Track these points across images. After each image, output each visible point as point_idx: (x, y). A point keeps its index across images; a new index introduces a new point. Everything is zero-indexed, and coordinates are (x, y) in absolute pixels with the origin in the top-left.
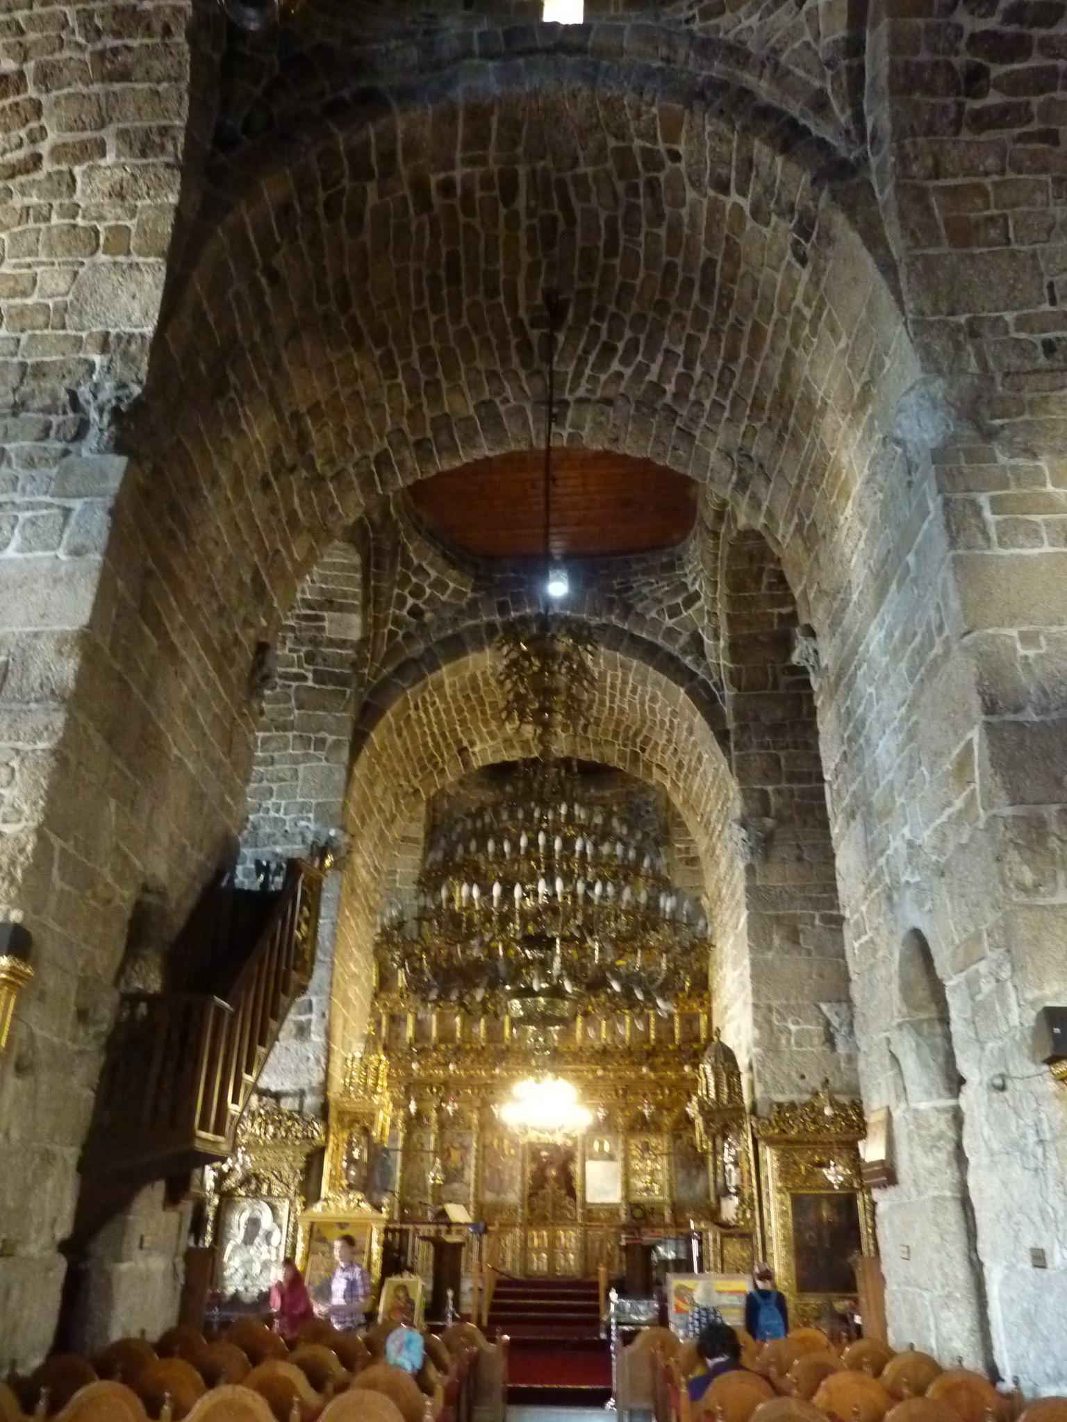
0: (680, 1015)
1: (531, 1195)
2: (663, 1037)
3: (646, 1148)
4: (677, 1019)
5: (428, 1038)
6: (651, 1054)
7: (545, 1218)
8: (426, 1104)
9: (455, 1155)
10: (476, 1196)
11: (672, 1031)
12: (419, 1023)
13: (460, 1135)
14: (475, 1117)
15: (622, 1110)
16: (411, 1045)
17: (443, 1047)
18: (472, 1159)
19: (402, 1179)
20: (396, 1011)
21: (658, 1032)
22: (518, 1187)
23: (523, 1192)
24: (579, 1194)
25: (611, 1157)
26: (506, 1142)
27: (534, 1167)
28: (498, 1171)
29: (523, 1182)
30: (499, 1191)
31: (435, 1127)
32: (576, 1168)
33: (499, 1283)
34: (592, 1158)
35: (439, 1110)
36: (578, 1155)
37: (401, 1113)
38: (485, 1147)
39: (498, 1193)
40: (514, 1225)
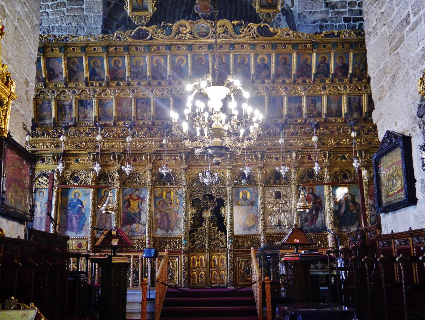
0: (307, 97)
1: (191, 232)
2: (293, 112)
3: (278, 196)
4: (304, 100)
5: (109, 118)
6: (285, 125)
7: (203, 246)
8: (112, 169)
9: (134, 204)
10: (150, 232)
11: (300, 109)
12: (101, 104)
13: (137, 190)
14: (148, 177)
15: (261, 169)
16: (95, 122)
17: (121, 123)
18: (146, 206)
19: (93, 222)
20: (83, 97)
21: (289, 109)
22: (182, 225)
23: (186, 229)
24: (228, 229)
25: (253, 203)
26: (172, 193)
27: (194, 211)
28: (167, 214)
29: (186, 221)
30: (168, 228)
31: (117, 184)
32: (226, 211)
33: (169, 294)
34: (237, 204)
35: (121, 172)
36: (228, 201)
37: (91, 175)
38: (156, 197)
39: (167, 231)
40: (180, 252)
